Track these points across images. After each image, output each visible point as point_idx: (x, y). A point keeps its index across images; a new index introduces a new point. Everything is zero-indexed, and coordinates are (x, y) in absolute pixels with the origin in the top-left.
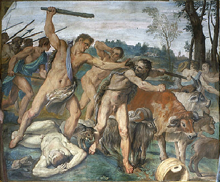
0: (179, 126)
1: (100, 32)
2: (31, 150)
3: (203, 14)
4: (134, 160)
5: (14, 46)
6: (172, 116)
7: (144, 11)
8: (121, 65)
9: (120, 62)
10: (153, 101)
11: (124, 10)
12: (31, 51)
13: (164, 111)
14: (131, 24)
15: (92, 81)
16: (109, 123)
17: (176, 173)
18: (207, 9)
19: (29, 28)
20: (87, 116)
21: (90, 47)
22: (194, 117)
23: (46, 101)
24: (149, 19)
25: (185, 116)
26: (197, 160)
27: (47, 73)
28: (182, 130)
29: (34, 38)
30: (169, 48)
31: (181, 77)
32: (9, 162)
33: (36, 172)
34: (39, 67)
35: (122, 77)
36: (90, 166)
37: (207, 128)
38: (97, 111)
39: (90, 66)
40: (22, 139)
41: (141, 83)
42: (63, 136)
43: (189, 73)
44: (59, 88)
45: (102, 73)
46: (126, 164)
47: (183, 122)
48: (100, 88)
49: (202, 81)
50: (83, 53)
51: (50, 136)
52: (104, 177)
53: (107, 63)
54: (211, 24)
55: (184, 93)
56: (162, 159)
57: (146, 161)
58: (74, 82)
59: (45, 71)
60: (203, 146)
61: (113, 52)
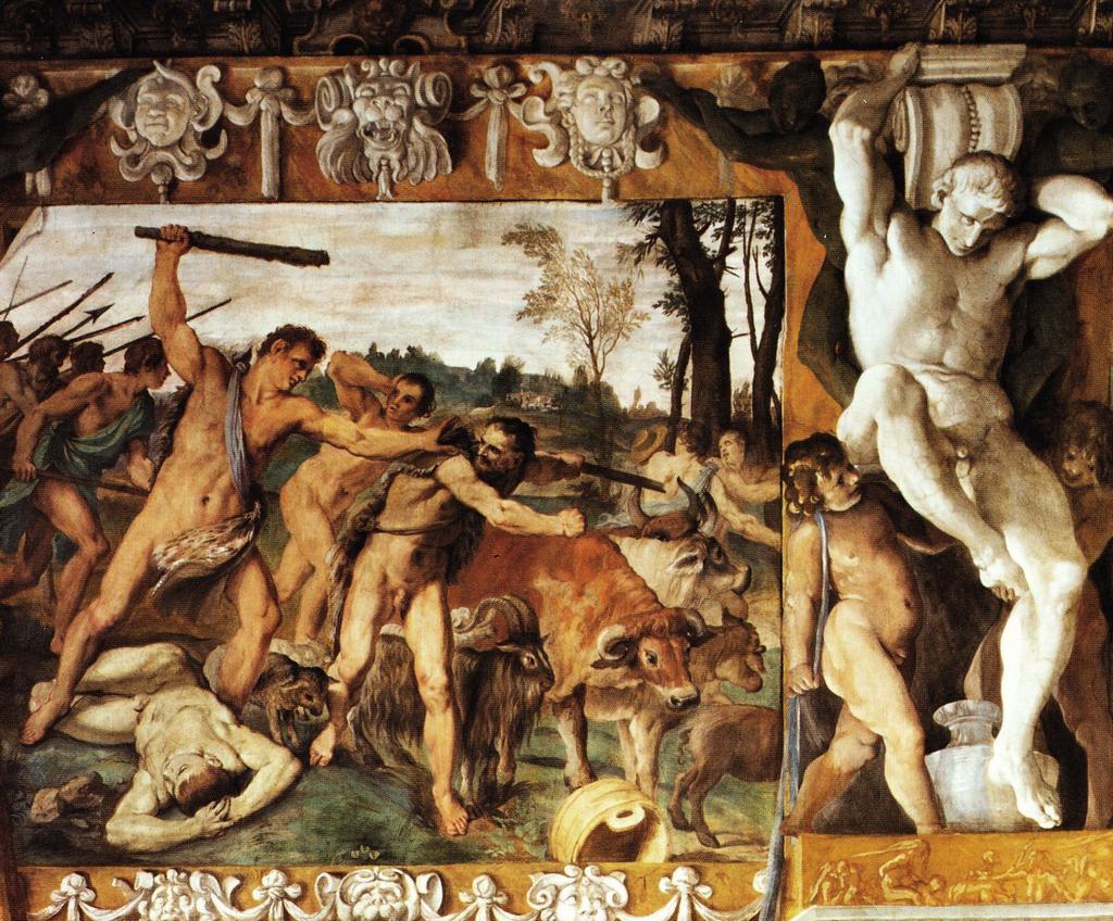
0: (634, 663)
1: (352, 318)
2: (102, 754)
3: (726, 250)
4: (470, 789)
5: (34, 370)
6: (609, 624)
7: (509, 238)
8: (426, 441)
9: (420, 430)
10: (542, 571)
11: (436, 239)
12: (96, 388)
13: (579, 608)
14: (463, 289)
15: (322, 501)
16: (380, 652)
17: (620, 835)
18: (740, 232)
19: (91, 304)
20: (303, 626)
21: (314, 375)
22: (691, 628)
23: (152, 573)
24: (527, 270)
25: (655, 627)
26: (701, 784)
27: (156, 471)
28: (646, 676)
29: (110, 341)
30: (599, 375)
31: (641, 483)
32: (20, 795)
33: (117, 833)
34: (126, 447)
35: (430, 482)
36: (313, 810)
37: (736, 669)
38: (336, 607)
39: (306, 442)
40: (66, 714)
41: (496, 505)
42: (213, 700)
43: (672, 467)
44: (200, 524)
45: (357, 468)
46: (444, 803)
47: (649, 646)
48: (349, 524)
49: (718, 496)
50: (286, 394)
51: (167, 700)
52: (365, 851)
53: (374, 433)
54: (754, 286)
55: (654, 543)
56: (574, 783)
57: (515, 791)
59: (147, 462)
60: (723, 734)
61: (395, 392)
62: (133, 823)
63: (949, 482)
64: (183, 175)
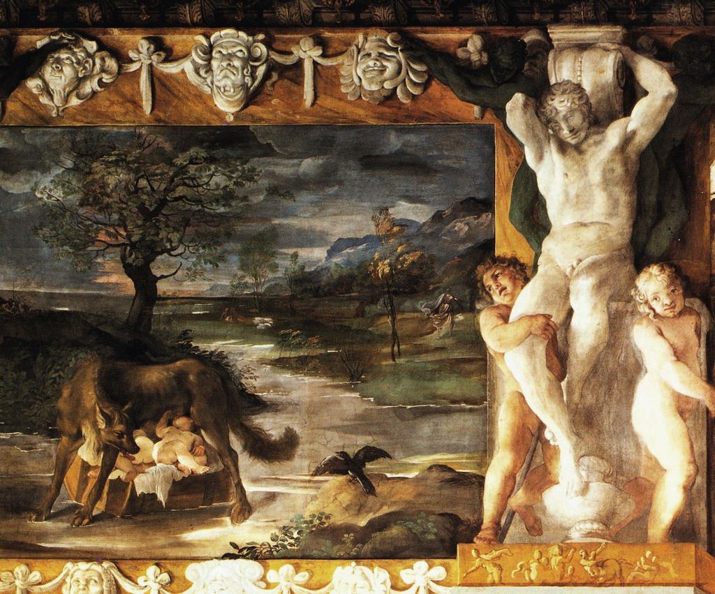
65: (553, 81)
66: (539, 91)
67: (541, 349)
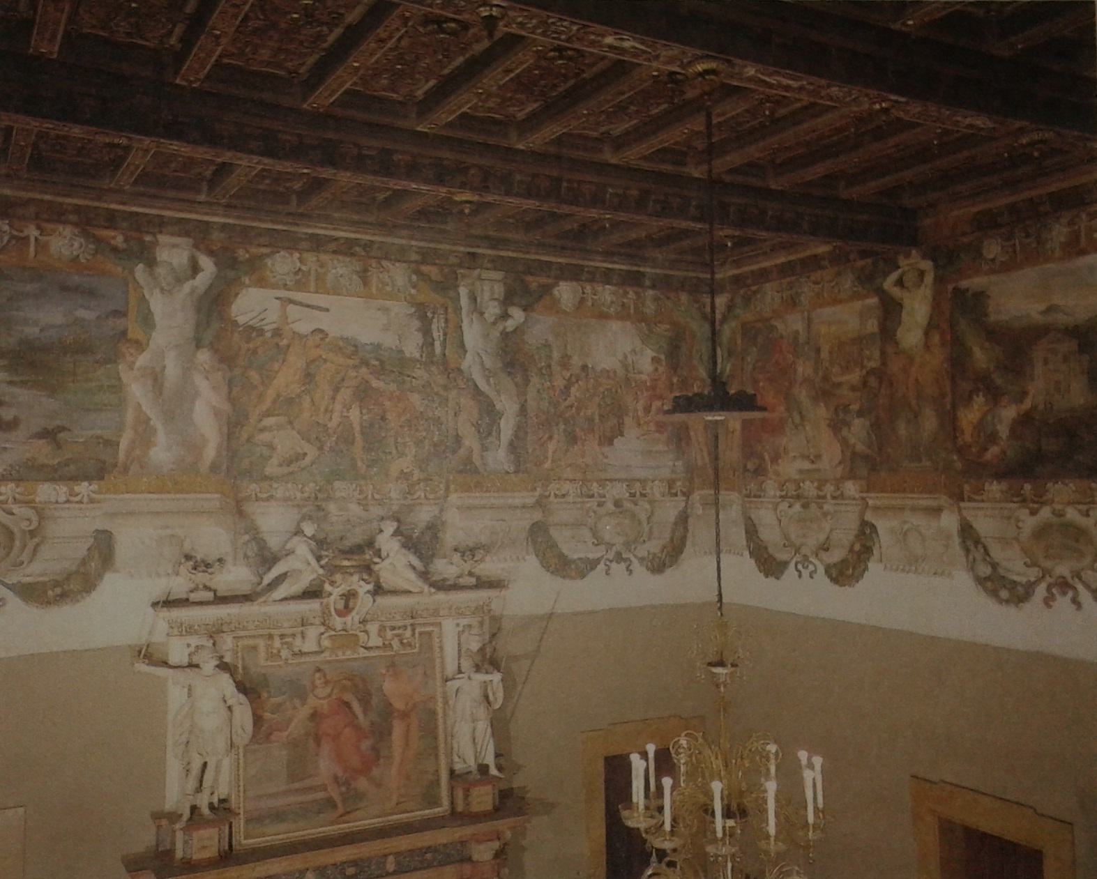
3: (433, 317)
19: (262, 317)
29: (266, 328)
58: (309, 377)
62: (272, 468)
63: (488, 381)
64: (288, 283)
65: (158, 259)
66: (151, 263)
67: (149, 382)
